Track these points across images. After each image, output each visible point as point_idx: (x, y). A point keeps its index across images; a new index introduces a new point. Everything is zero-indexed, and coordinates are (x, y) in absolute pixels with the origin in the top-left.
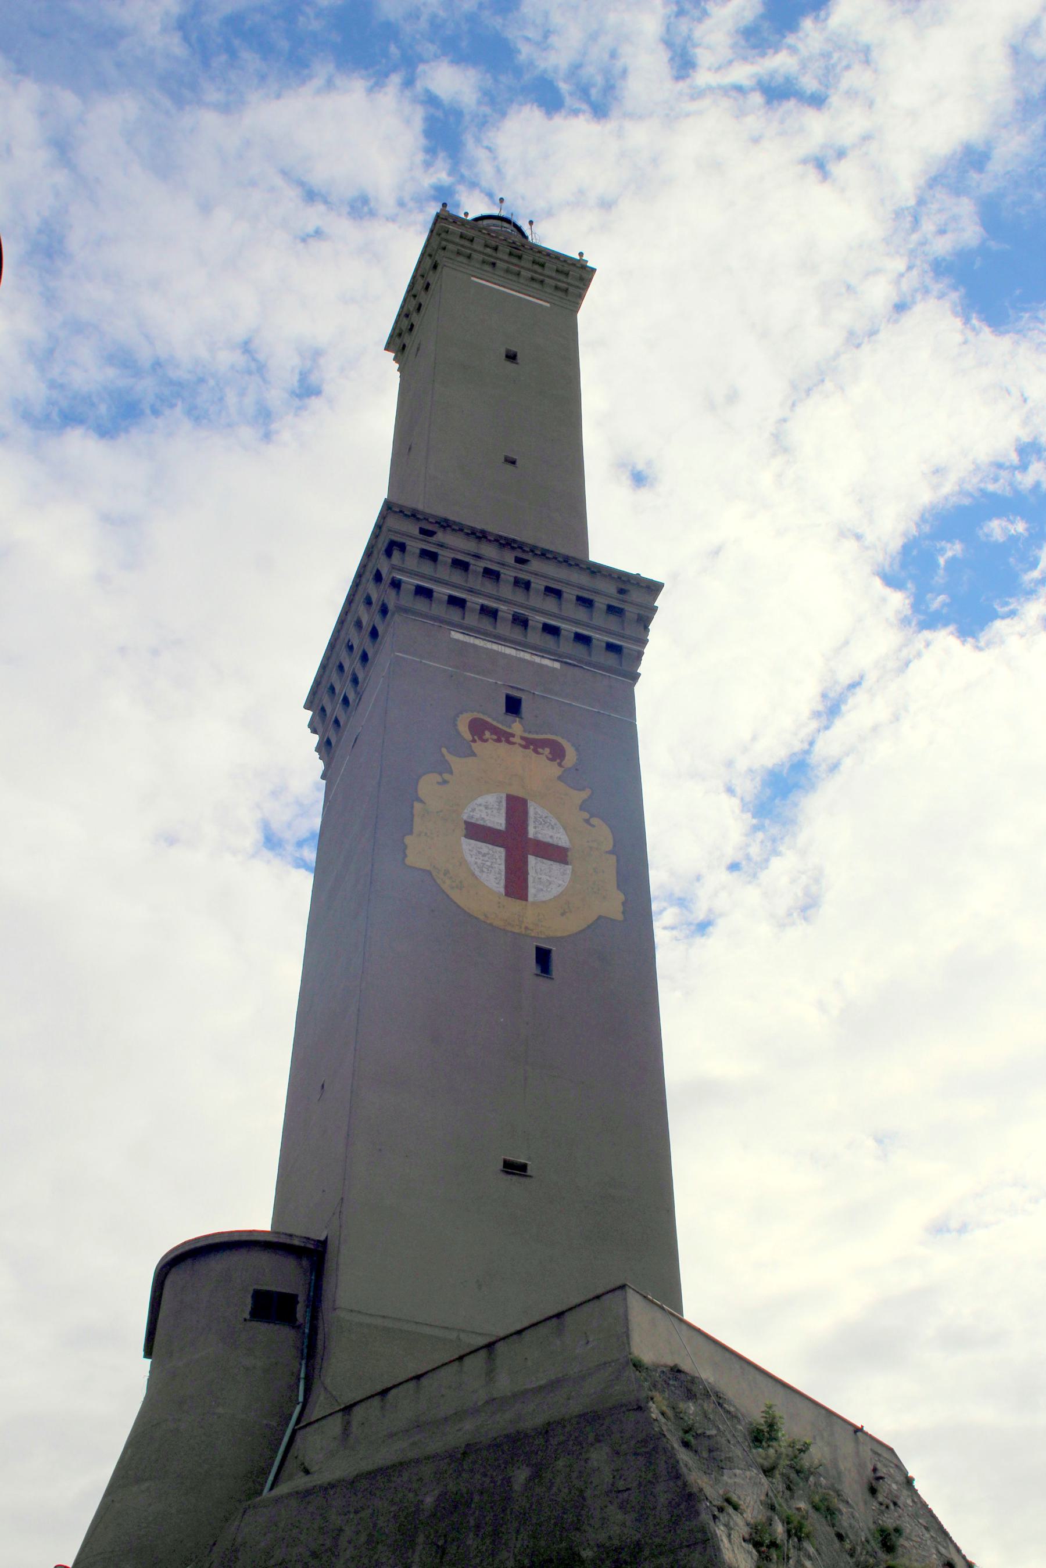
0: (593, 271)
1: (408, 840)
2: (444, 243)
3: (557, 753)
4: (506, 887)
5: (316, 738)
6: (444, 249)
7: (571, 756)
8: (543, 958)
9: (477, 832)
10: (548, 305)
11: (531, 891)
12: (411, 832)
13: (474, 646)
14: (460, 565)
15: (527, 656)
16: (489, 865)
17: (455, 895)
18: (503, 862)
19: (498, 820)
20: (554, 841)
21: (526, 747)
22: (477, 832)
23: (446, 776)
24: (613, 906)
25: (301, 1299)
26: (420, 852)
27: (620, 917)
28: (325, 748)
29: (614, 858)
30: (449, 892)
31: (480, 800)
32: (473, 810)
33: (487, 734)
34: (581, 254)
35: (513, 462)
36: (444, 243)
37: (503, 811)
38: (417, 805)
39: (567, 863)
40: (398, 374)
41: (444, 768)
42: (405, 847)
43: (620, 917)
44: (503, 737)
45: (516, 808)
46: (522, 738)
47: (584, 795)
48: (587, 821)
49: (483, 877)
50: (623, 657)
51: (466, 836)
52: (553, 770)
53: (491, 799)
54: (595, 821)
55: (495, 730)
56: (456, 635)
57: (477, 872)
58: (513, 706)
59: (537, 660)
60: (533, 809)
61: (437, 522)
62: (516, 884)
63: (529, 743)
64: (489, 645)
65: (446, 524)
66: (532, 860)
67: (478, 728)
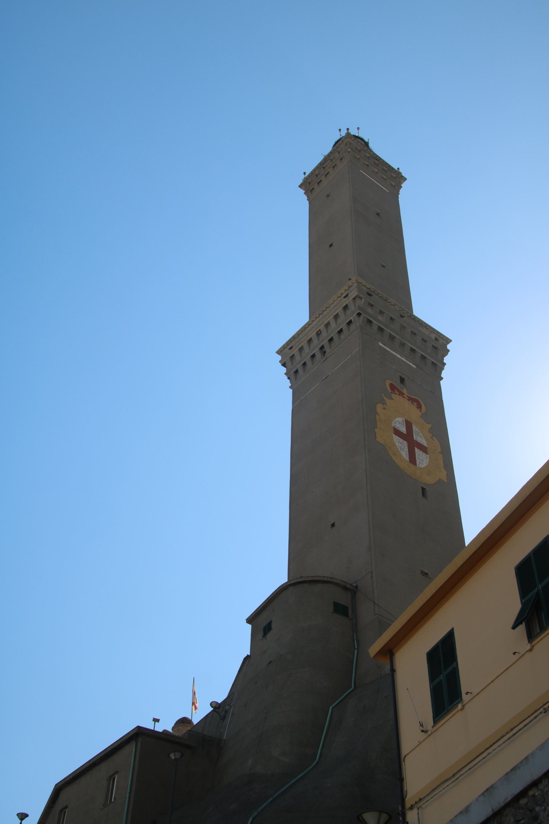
0: (406, 179)
1: (376, 430)
2: (349, 150)
3: (419, 407)
4: (410, 458)
5: (284, 370)
6: (349, 152)
8: (423, 489)
9: (397, 432)
11: (418, 463)
12: (377, 428)
13: (388, 351)
14: (381, 312)
15: (405, 360)
17: (393, 457)
18: (407, 447)
19: (403, 430)
20: (422, 443)
21: (409, 400)
22: (397, 432)
23: (385, 406)
24: (443, 476)
25: (350, 608)
27: (446, 481)
28: (293, 375)
29: (441, 455)
30: (392, 456)
31: (397, 419)
32: (395, 423)
33: (396, 392)
34: (398, 169)
35: (384, 267)
36: (349, 150)
37: (405, 426)
38: (377, 416)
39: (427, 454)
40: (308, 202)
41: (384, 403)
42: (376, 433)
43: (446, 481)
44: (401, 394)
45: (409, 425)
46: (407, 396)
47: (429, 426)
48: (432, 437)
49: (402, 452)
51: (395, 434)
53: (400, 419)
54: (434, 438)
55: (398, 390)
56: (381, 344)
57: (399, 449)
58: (402, 380)
59: (408, 362)
60: (414, 428)
61: (374, 292)
62: (413, 459)
63: (410, 399)
64: (392, 352)
66: (416, 450)
67: (392, 387)
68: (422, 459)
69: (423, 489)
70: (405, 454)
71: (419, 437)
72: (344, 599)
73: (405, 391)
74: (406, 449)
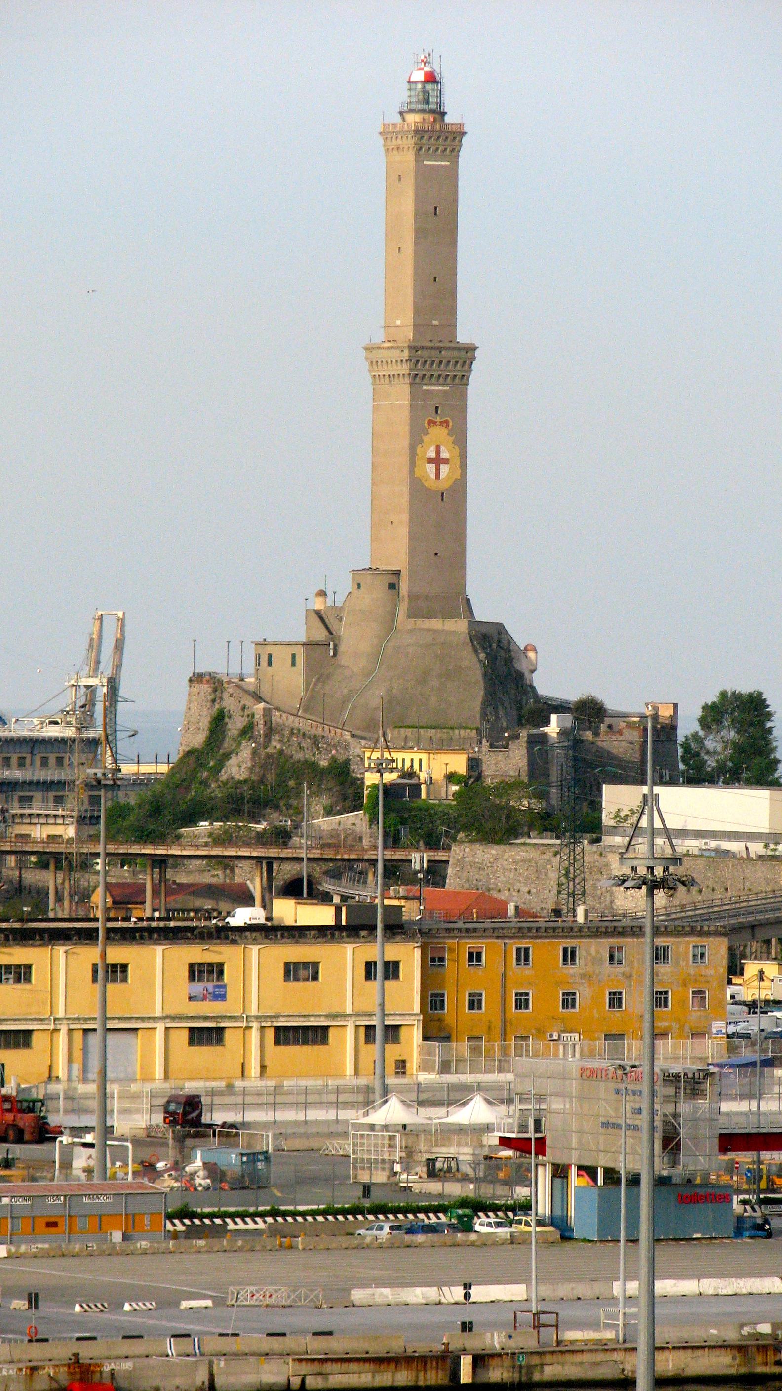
7: (451, 424)
9: (430, 461)
10: (448, 163)
16: (431, 469)
19: (432, 455)
22: (430, 461)
26: (418, 473)
41: (422, 441)
44: (435, 423)
50: (464, 380)
52: (446, 431)
54: (456, 447)
56: (424, 388)
60: (442, 448)
65: (422, 348)
67: (430, 423)
68: (445, 469)
69: (443, 494)
70: (433, 476)
71: (445, 455)
72: (393, 580)
73: (438, 420)
74: (434, 470)
